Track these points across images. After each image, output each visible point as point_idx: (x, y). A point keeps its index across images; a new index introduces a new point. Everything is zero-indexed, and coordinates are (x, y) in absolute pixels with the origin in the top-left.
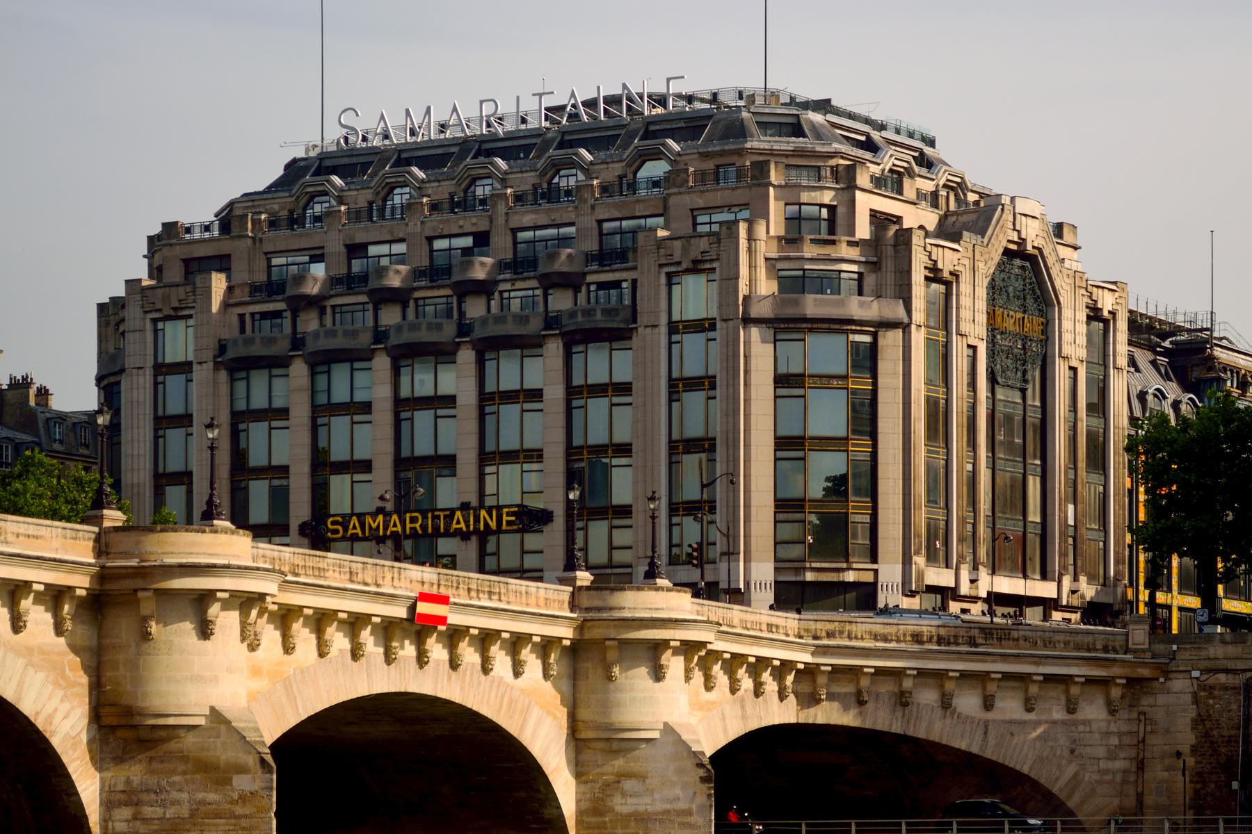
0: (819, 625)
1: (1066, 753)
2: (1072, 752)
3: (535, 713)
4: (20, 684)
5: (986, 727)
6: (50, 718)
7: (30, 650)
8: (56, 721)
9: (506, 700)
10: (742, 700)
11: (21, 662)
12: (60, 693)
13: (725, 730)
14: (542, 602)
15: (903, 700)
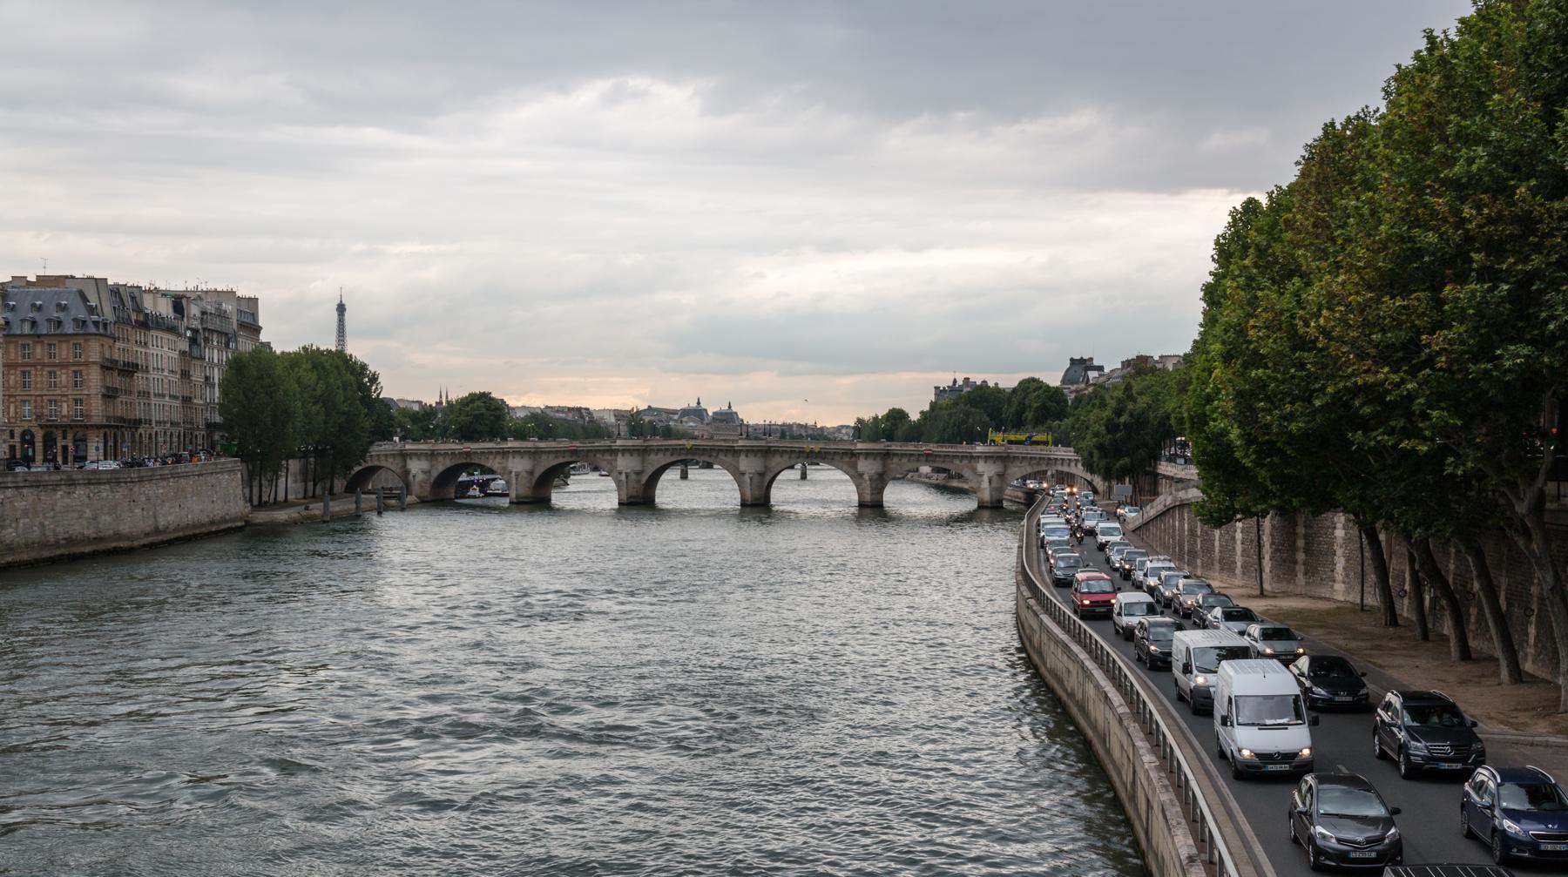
15: (1069, 465)
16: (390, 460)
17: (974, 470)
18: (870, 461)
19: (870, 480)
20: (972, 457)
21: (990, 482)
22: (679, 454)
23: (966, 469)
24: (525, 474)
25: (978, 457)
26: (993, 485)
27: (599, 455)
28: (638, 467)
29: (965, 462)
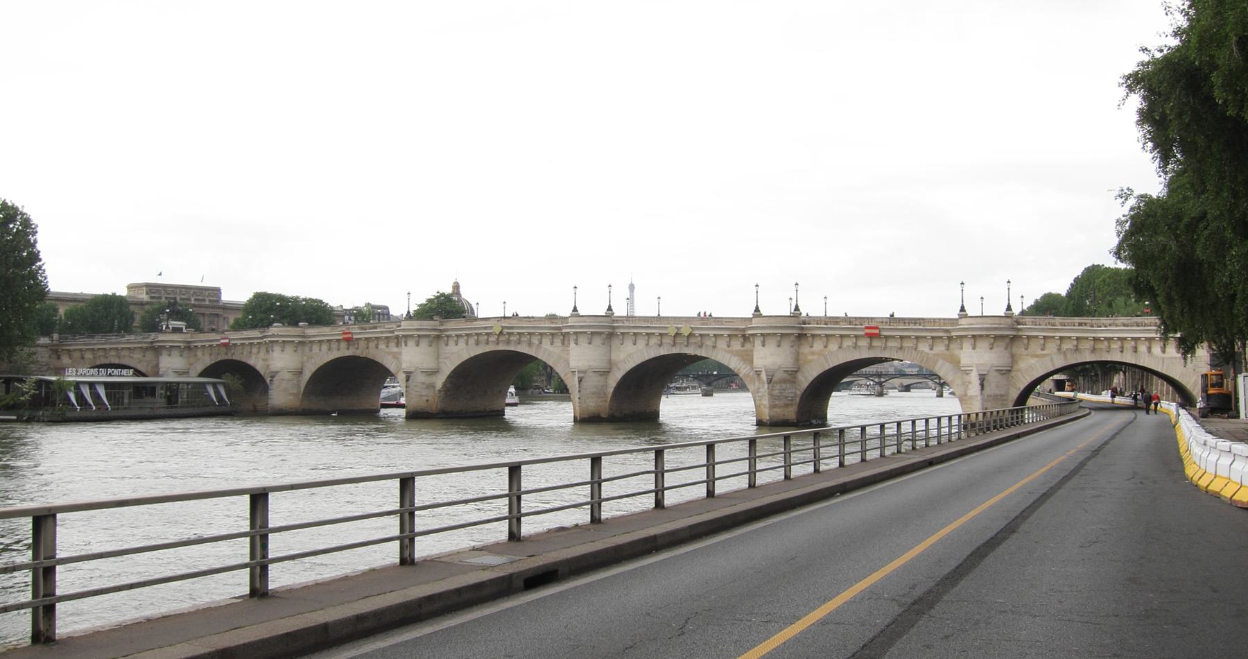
0: (1107, 322)
1: (1192, 371)
2: (1194, 370)
3: (940, 362)
4: (729, 361)
5: (1163, 360)
6: (739, 369)
7: (732, 351)
8: (741, 369)
9: (925, 359)
10: (1065, 353)
11: (729, 355)
12: (742, 363)
13: (1053, 365)
14: (942, 324)
15: (1135, 350)
16: (137, 355)
17: (956, 363)
18: (771, 346)
19: (770, 382)
20: (950, 338)
21: (982, 385)
22: (487, 343)
23: (940, 362)
24: (288, 376)
25: (961, 337)
26: (987, 391)
27: (382, 346)
28: (429, 364)
29: (940, 348)
